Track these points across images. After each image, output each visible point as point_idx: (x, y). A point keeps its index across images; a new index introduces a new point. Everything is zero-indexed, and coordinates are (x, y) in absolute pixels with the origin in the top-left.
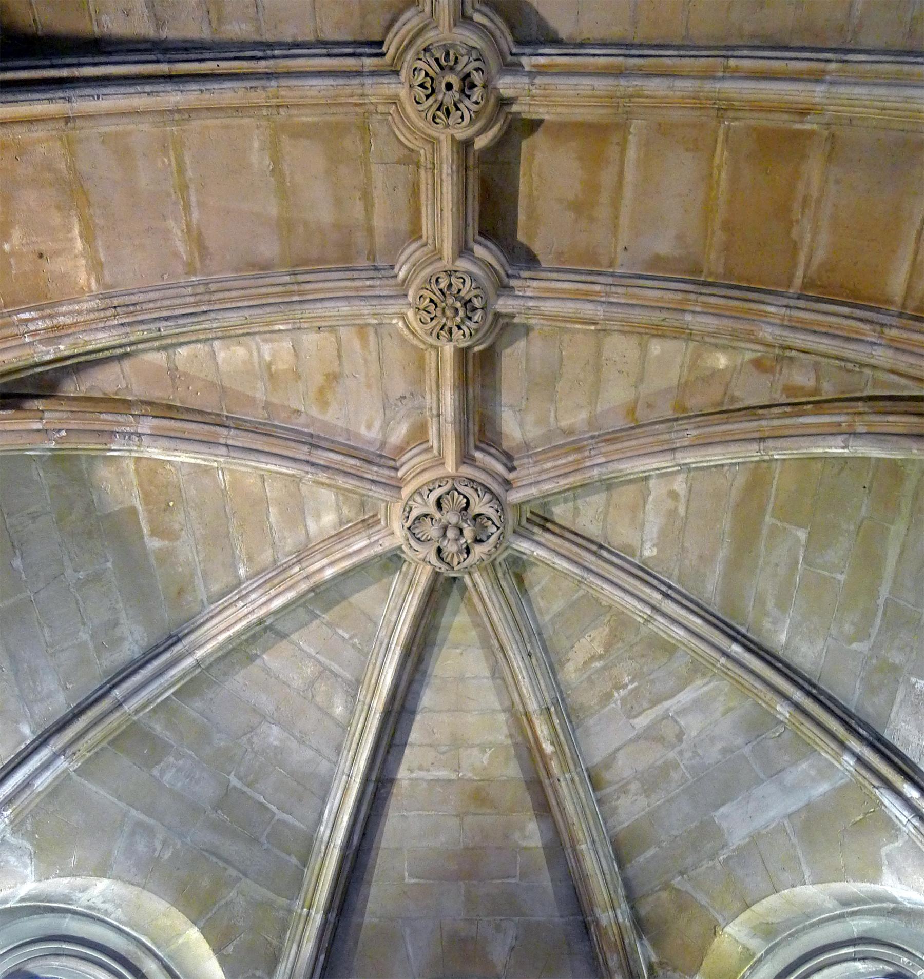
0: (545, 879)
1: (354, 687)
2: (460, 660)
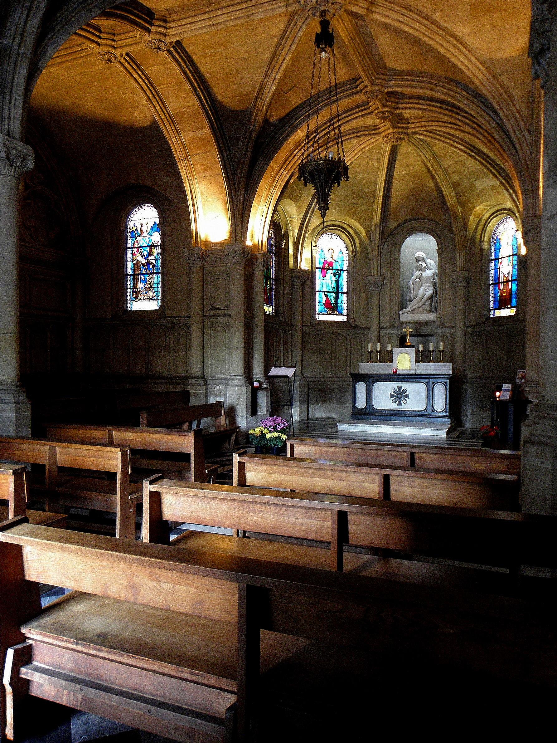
0: (435, 193)
1: (378, 160)
2: (405, 148)
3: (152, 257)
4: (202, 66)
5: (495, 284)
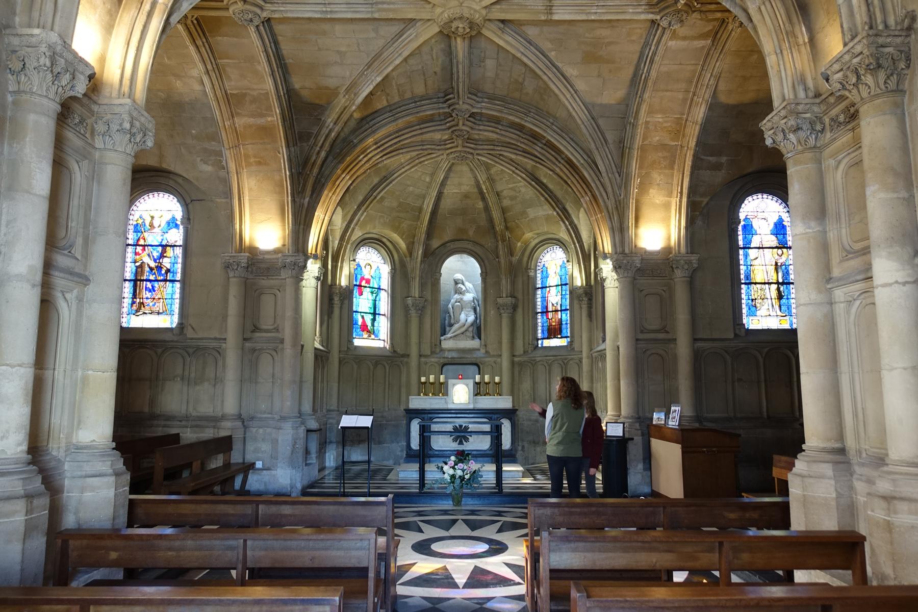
0: (484, 215)
3: (165, 260)
4: (286, 48)
5: (542, 313)
